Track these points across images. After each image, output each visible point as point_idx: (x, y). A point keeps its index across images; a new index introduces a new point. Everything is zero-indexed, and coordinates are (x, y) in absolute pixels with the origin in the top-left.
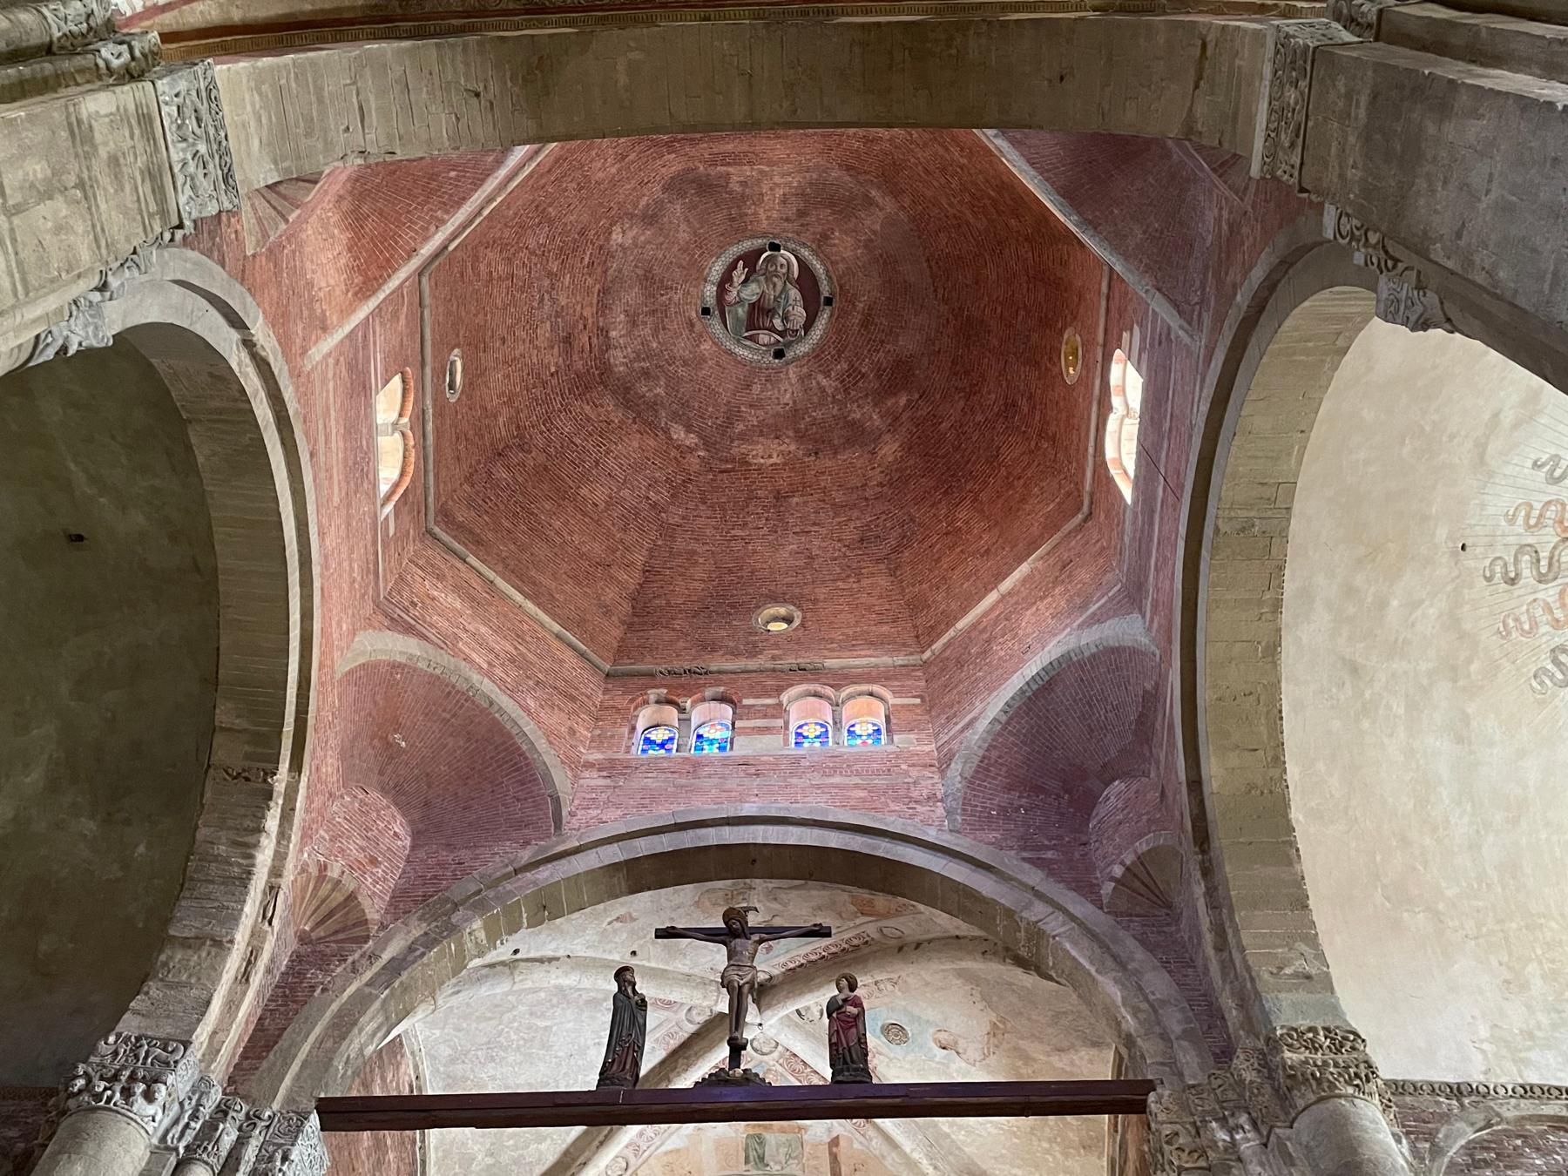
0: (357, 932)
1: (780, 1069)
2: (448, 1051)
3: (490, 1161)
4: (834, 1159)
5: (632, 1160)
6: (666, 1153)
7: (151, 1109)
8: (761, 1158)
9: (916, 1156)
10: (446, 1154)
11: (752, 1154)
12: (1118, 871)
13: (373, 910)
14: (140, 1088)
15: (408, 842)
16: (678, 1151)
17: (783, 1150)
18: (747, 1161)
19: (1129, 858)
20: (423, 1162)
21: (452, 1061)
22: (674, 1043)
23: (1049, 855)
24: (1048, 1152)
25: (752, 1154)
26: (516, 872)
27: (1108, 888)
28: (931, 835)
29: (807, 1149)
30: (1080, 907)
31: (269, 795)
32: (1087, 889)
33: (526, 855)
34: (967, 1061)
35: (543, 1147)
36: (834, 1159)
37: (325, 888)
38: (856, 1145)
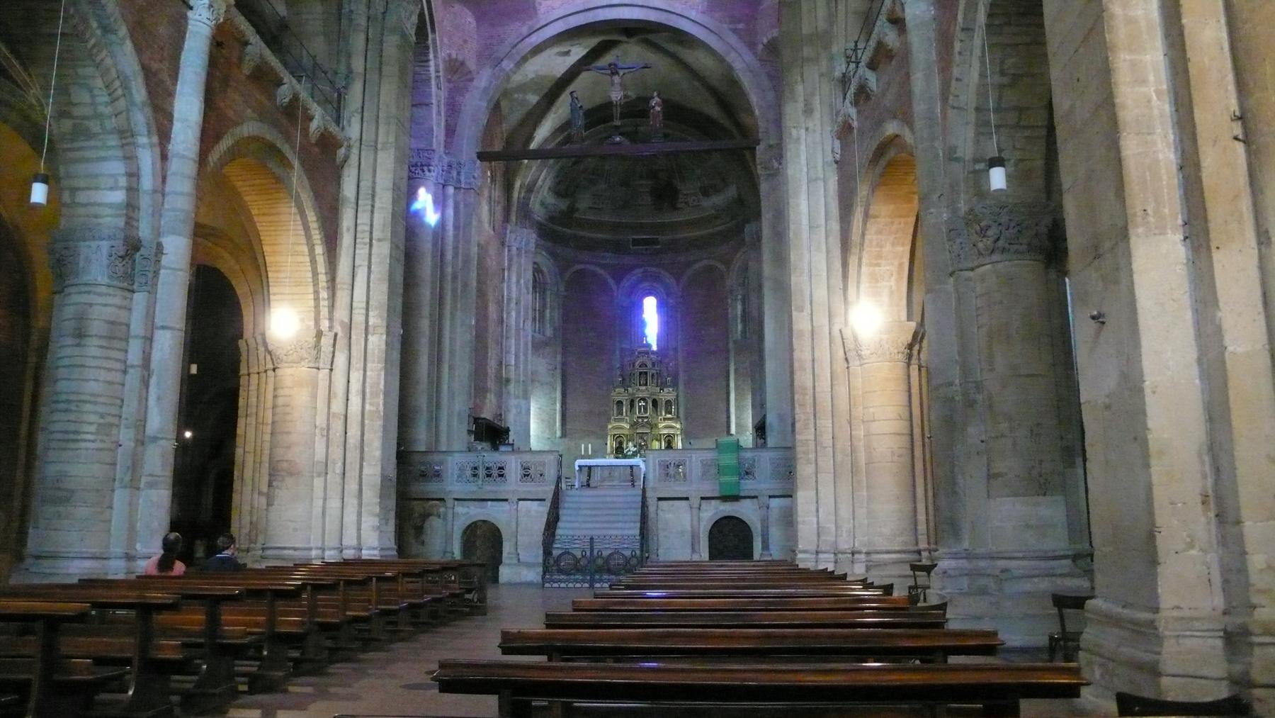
0: (469, 77)
7: (433, 174)
12: (765, 41)
13: (472, 64)
14: (425, 168)
15: (474, 24)
19: (770, 37)
23: (741, 26)
26: (522, 40)
27: (760, 47)
28: (693, 15)
30: (749, 57)
31: (427, 48)
32: (752, 45)
33: (525, 30)
37: (452, 64)
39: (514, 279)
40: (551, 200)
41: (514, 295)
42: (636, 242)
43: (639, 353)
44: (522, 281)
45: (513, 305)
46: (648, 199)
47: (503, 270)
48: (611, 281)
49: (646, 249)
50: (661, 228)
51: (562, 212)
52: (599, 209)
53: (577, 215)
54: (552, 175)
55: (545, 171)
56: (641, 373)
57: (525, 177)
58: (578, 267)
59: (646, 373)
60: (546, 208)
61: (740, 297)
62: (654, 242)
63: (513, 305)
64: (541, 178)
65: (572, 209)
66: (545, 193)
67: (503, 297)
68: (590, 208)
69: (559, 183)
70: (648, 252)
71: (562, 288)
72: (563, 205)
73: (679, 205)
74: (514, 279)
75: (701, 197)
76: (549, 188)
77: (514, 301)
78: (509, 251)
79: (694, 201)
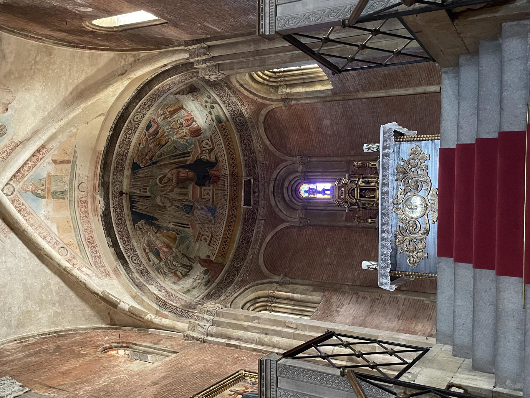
1: (21, 184)
2: (5, 328)
3: (57, 304)
4: (62, 162)
5: (60, 246)
6: (59, 232)
8: (62, 192)
9: (57, 127)
10: (53, 323)
11: (61, 196)
16: (58, 227)
17: (59, 183)
18: (64, 199)
20: (55, 332)
21: (9, 326)
22: (7, 229)
24: (53, 71)
25: (61, 196)
29: (58, 173)
34: (13, 100)
35: (52, 283)
36: (62, 162)
38: (56, 152)
39: (240, 333)
40: (188, 283)
41: (256, 336)
42: (247, 203)
43: (339, 198)
44: (245, 323)
45: (266, 338)
46: (208, 189)
47: (228, 345)
48: (280, 227)
49: (254, 192)
50: (234, 175)
51: (205, 273)
52: (212, 236)
53: (213, 258)
54: (160, 280)
55: (149, 287)
56: (361, 196)
57: (150, 308)
58: (261, 262)
59: (361, 190)
60: (194, 288)
61: (288, 91)
62: (248, 183)
63: (266, 338)
64: (156, 292)
65: (206, 262)
66: (176, 287)
67: (255, 350)
68: (209, 245)
69: (175, 275)
70: (257, 190)
71: (276, 278)
72: (198, 271)
73: (213, 160)
74: (240, 333)
75: (202, 136)
76: (174, 283)
77: (263, 336)
78: (211, 335)
79: (207, 144)
